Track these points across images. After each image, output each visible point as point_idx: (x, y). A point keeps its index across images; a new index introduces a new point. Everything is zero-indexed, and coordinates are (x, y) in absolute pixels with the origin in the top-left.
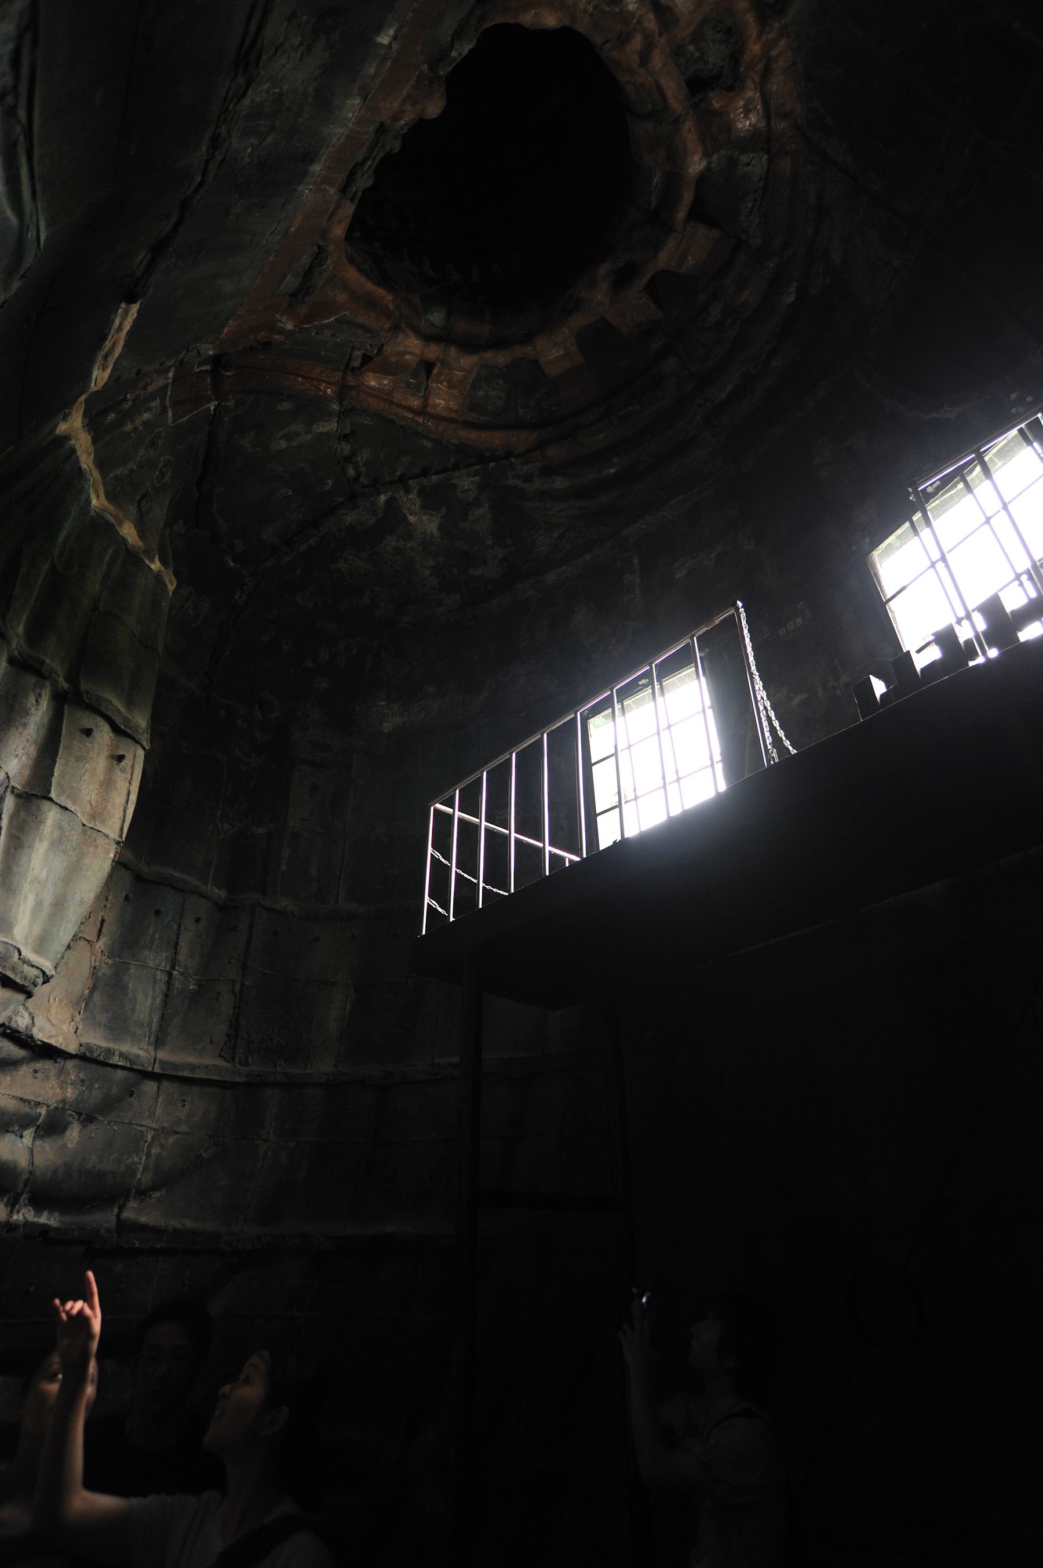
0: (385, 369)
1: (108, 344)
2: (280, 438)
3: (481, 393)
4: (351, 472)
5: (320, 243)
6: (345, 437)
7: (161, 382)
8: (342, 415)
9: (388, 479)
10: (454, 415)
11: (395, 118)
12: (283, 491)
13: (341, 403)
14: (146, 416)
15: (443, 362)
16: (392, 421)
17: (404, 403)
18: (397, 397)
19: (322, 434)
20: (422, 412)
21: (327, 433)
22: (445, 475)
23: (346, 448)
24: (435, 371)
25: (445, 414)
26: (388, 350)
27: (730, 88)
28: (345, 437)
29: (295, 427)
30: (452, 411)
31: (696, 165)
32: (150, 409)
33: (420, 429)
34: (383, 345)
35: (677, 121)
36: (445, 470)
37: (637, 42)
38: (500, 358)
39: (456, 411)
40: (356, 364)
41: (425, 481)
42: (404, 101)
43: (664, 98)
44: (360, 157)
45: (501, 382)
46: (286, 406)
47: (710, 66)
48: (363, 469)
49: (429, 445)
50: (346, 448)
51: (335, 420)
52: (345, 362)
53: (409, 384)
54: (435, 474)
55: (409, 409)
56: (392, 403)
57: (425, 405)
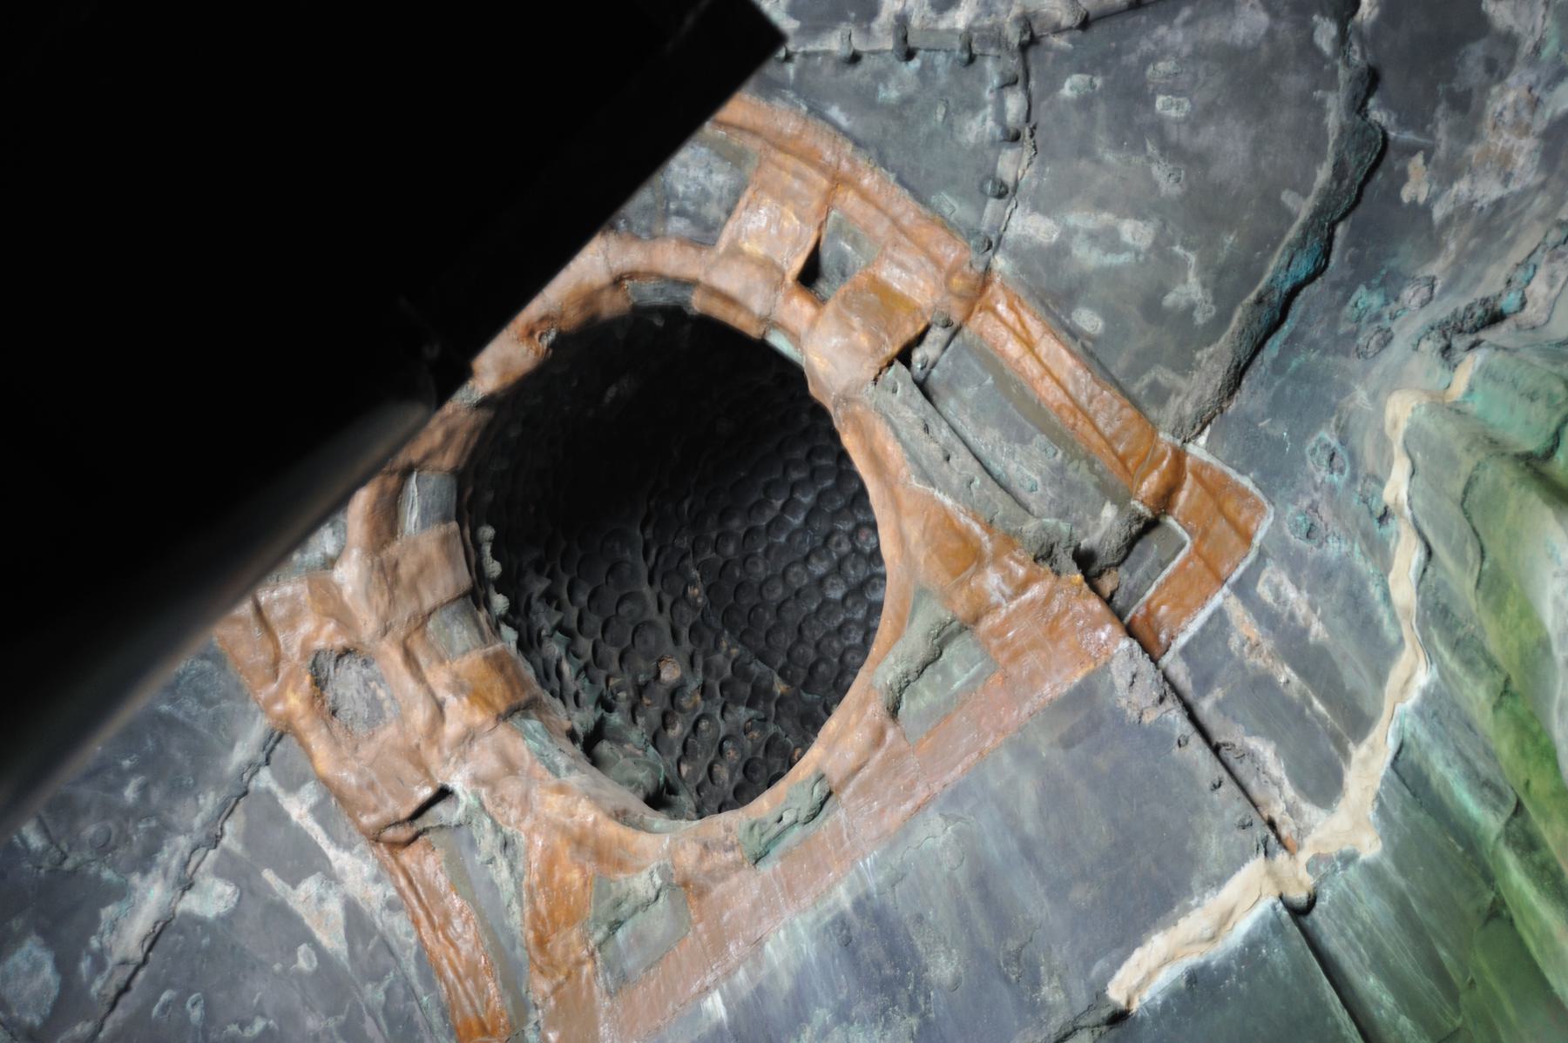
0: (885, 302)
1: (1193, 959)
2: (1125, 248)
3: (719, 178)
4: (1014, 104)
5: (890, 723)
6: (1003, 192)
7: (1236, 610)
8: (991, 245)
9: (940, 58)
10: (780, 157)
11: (738, 866)
12: (1173, 113)
13: (988, 269)
14: (1291, 593)
15: (777, 285)
16: (901, 181)
17: (872, 211)
18: (882, 228)
19: (1046, 213)
20: (838, 180)
21: (1035, 208)
22: (810, 48)
23: (1009, 165)
24: (798, 263)
25: (790, 162)
26: (868, 370)
27: (318, 653)
28: (1003, 192)
29: (1088, 257)
30: (781, 167)
31: (350, 575)
32: (1277, 595)
33: (849, 147)
34: (876, 380)
35: (385, 631)
36: (806, 55)
37: (452, 729)
38: (671, 259)
39: (772, 162)
40: (937, 335)
41: (858, 44)
42: (724, 878)
43: (409, 658)
44: (797, 829)
45: (680, 188)
46: (1088, 320)
47: (354, 667)
48: (988, 96)
49: (835, 112)
50: (1009, 165)
51: (1010, 235)
52: (957, 340)
53: (855, 242)
54: (827, 54)
55: (864, 196)
56: (895, 221)
57: (828, 202)
